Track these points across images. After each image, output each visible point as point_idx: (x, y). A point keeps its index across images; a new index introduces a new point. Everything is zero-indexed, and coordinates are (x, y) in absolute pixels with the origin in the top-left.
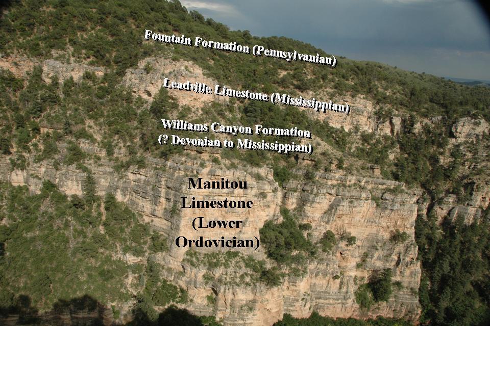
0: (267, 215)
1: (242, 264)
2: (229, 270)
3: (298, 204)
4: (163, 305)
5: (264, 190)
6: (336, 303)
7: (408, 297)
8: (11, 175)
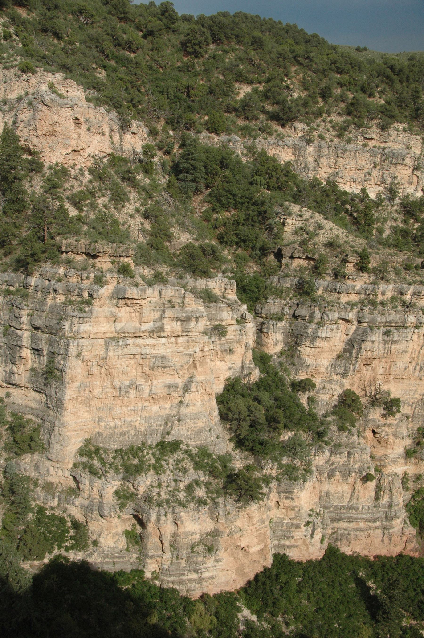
0: (230, 368)
1: (189, 465)
2: (164, 478)
3: (286, 344)
4: (40, 557)
6: (370, 528)
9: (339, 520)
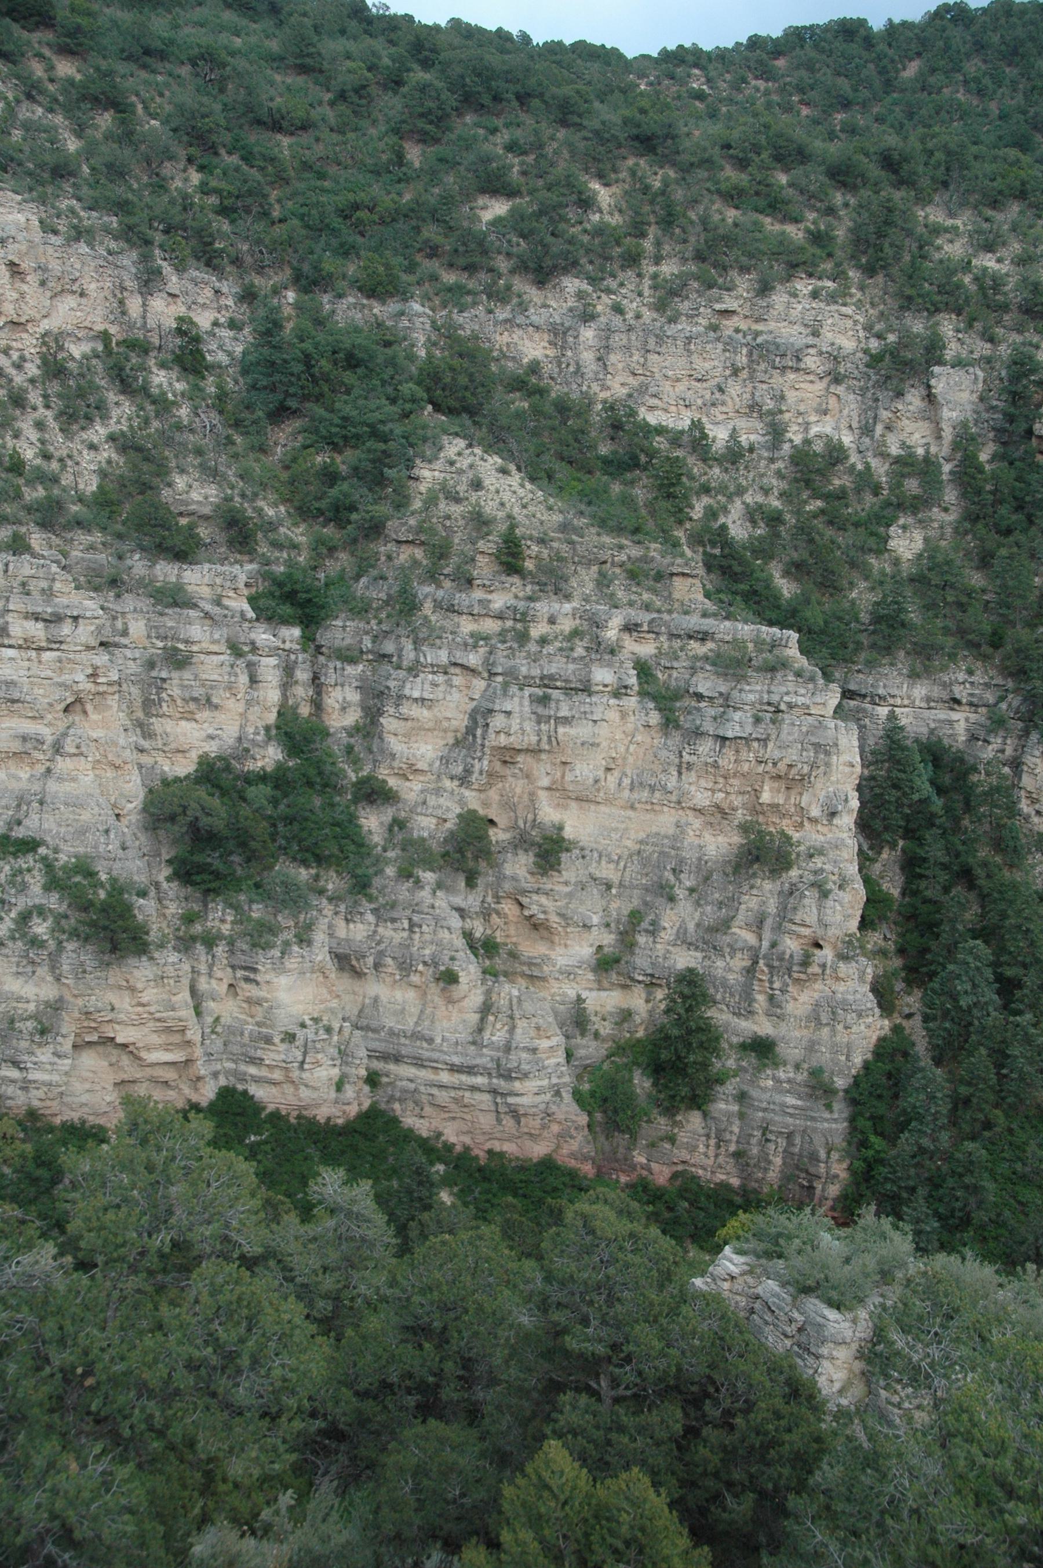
0: (211, 737)
1: (36, 882)
5: (186, 642)
7: (791, 1100)
9: (397, 1059)
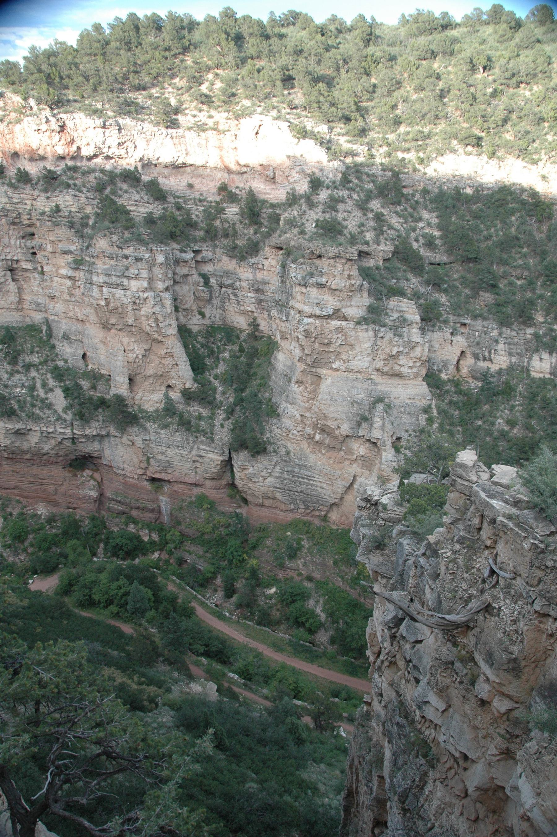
8: (530, 359)
